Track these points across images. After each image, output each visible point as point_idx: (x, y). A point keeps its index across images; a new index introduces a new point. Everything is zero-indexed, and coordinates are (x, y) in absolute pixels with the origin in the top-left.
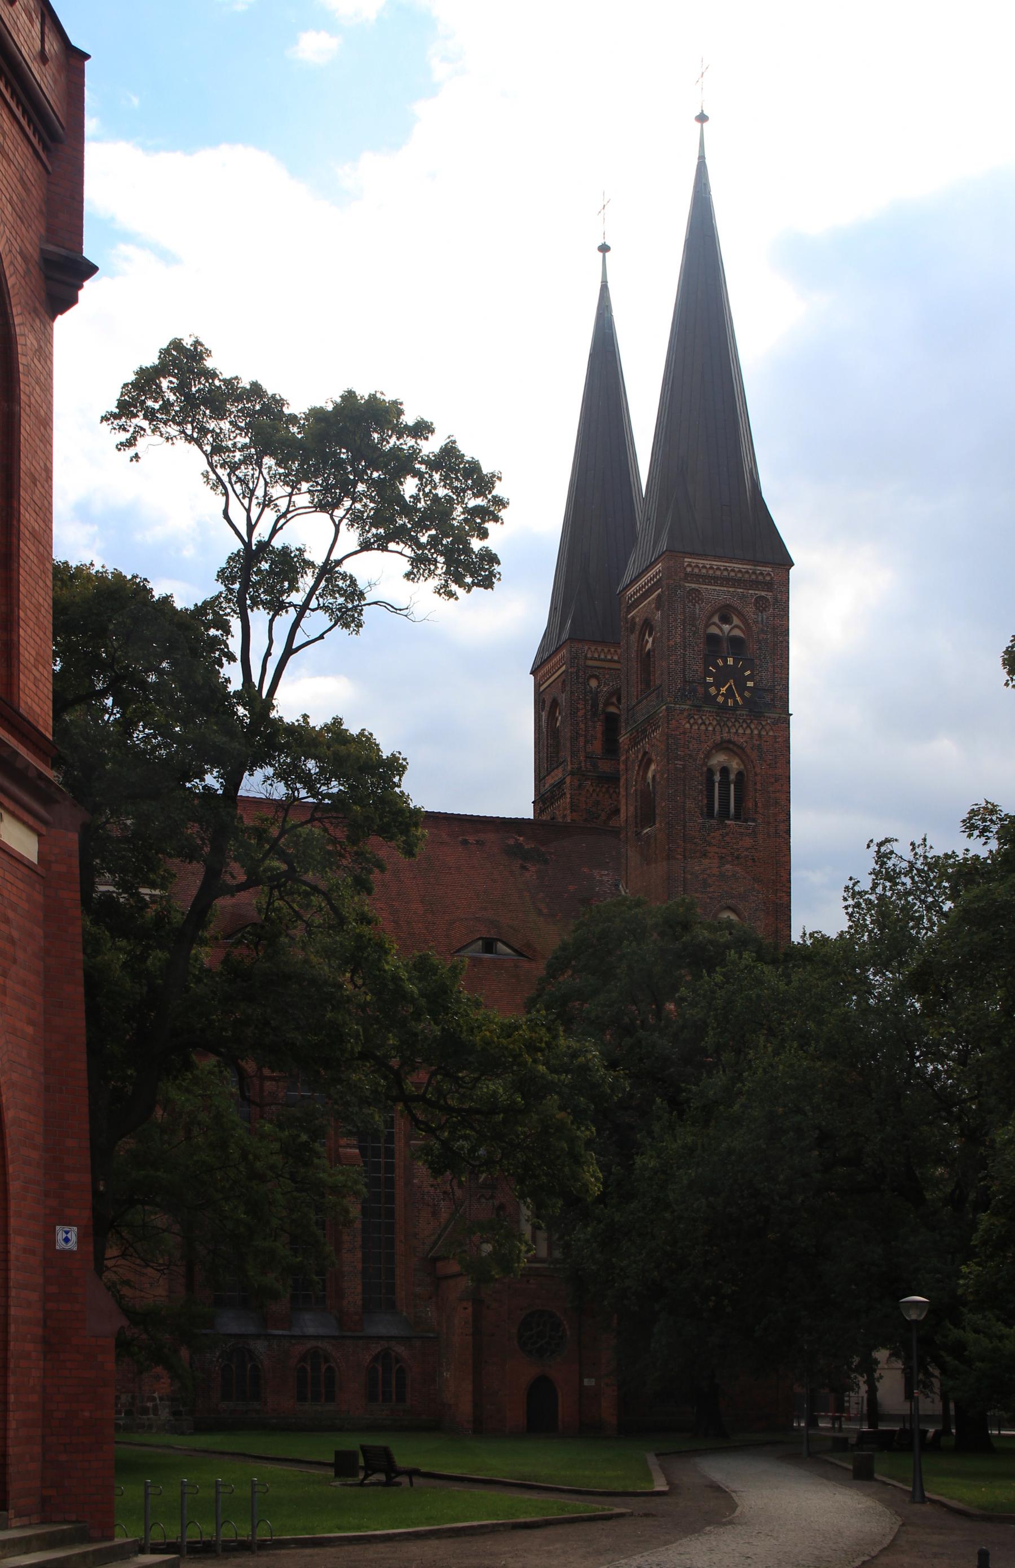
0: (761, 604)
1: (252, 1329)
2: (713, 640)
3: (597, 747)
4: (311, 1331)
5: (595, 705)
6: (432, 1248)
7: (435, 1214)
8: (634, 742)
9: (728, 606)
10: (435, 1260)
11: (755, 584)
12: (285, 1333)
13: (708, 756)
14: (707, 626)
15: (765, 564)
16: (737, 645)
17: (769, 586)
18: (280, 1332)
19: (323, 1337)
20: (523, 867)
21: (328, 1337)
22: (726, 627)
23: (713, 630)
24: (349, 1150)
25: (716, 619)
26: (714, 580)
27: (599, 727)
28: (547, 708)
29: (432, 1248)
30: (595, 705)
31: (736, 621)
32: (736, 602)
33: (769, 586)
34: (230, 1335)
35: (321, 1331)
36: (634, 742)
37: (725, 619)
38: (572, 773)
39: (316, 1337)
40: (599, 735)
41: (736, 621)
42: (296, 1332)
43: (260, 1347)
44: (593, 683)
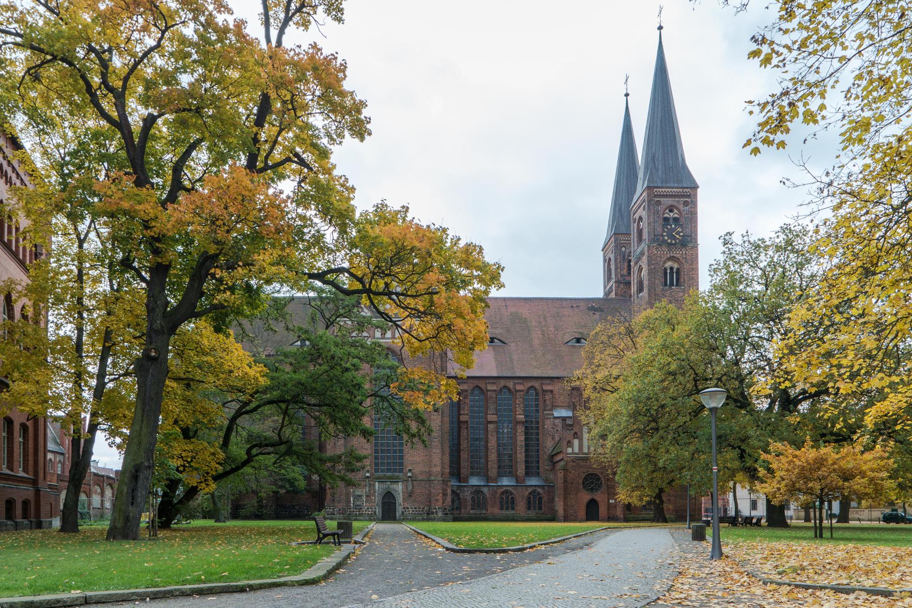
3: (625, 272)
4: (505, 484)
8: (636, 263)
9: (672, 206)
11: (683, 196)
13: (665, 263)
15: (687, 188)
16: (676, 220)
22: (671, 214)
26: (666, 196)
31: (676, 211)
32: (675, 204)
33: (689, 196)
35: (509, 484)
36: (636, 263)
37: (671, 211)
41: (676, 211)
44: (623, 249)
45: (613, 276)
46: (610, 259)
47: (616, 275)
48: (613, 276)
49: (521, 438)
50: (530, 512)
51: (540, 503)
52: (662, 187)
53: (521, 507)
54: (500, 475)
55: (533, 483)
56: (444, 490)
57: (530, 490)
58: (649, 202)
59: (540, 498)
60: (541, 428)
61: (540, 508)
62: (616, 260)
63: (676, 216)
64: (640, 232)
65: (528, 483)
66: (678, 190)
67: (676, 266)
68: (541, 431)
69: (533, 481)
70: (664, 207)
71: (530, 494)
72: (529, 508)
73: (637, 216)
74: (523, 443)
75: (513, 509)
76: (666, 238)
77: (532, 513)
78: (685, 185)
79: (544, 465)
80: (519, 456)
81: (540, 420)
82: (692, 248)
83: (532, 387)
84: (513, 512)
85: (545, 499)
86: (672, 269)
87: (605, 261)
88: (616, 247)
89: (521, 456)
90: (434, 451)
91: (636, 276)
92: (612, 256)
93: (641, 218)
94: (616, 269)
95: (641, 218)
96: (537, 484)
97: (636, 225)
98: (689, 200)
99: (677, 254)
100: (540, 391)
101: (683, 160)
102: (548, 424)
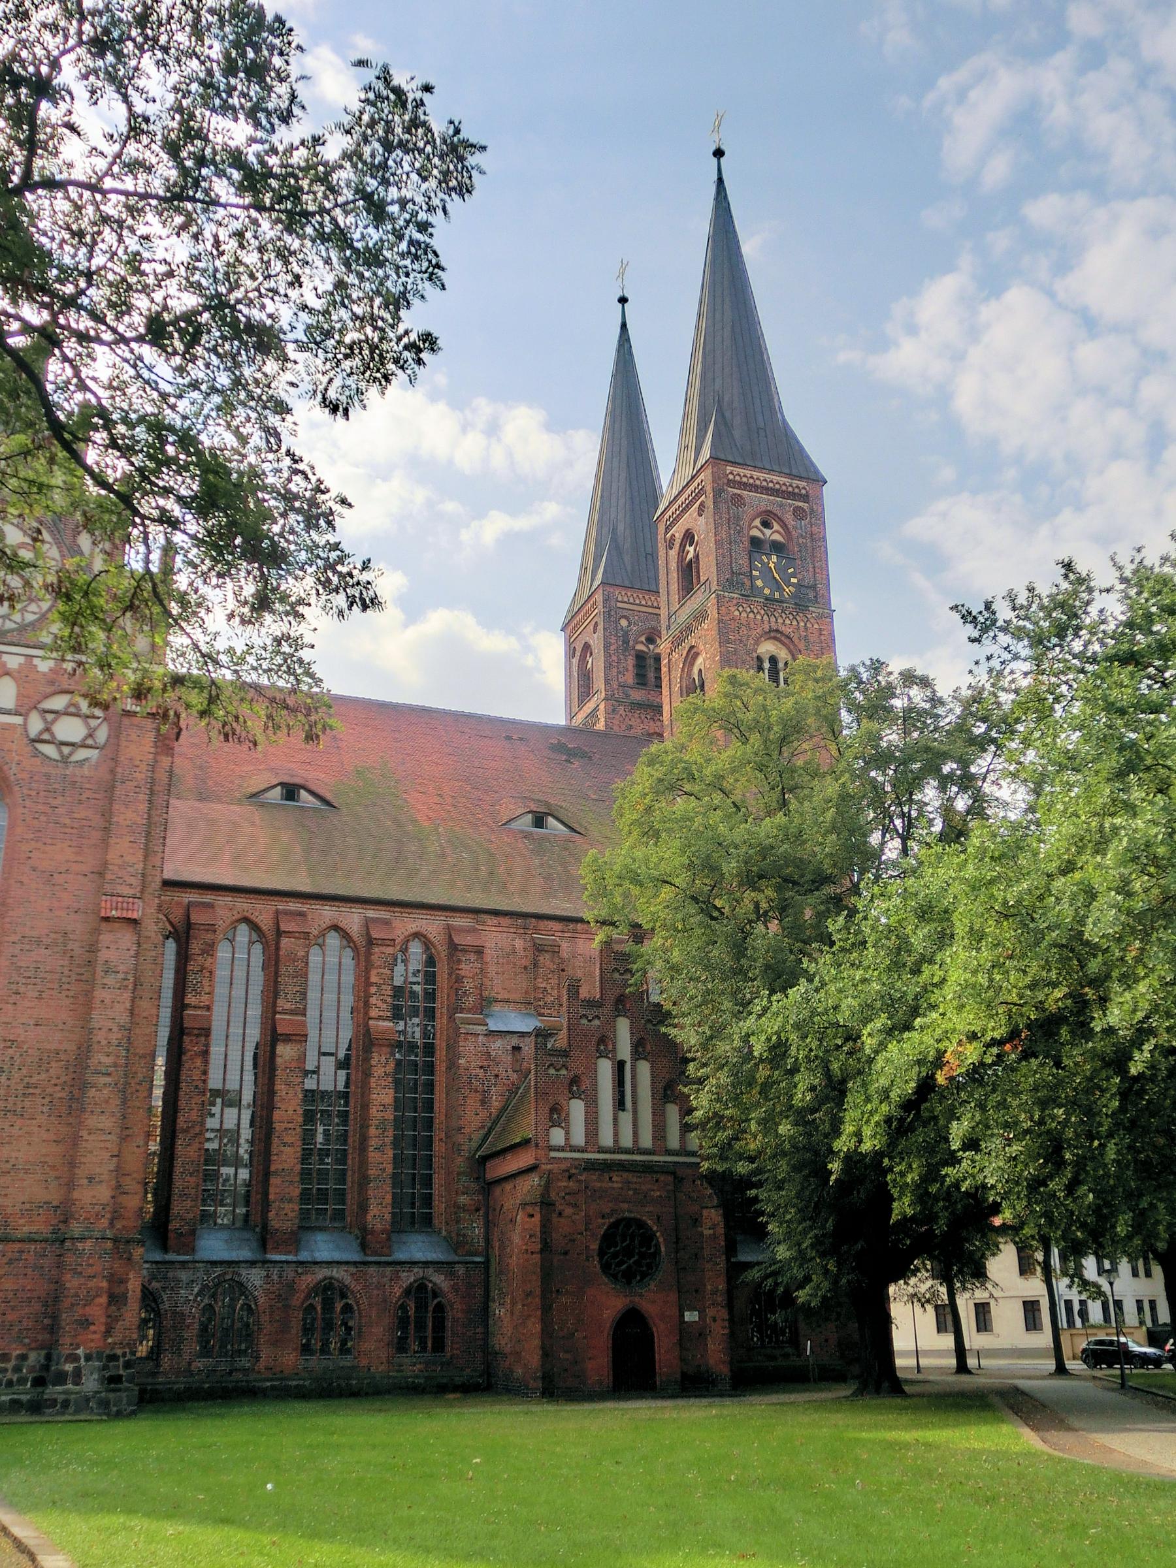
0: (799, 513)
1: (245, 1254)
2: (756, 542)
3: (629, 678)
5: (626, 642)
6: (481, 1146)
7: (483, 1102)
8: (677, 642)
9: (769, 512)
10: (485, 1159)
11: (792, 495)
12: (290, 1258)
14: (750, 528)
15: (801, 478)
16: (777, 547)
17: (805, 498)
18: (283, 1258)
19: (338, 1263)
20: (567, 761)
21: (347, 1263)
22: (768, 532)
23: (755, 532)
24: (381, 1023)
25: (757, 522)
26: (755, 488)
27: (631, 661)
28: (578, 654)
29: (481, 1146)
30: (626, 642)
31: (776, 527)
32: (776, 510)
33: (805, 498)
34: (214, 1263)
35: (337, 1256)
36: (677, 642)
37: (766, 524)
38: (606, 699)
39: (329, 1263)
40: (631, 668)
41: (776, 527)
42: (304, 1256)
43: (255, 1278)
44: (624, 623)
45: (599, 683)
46: (587, 647)
47: (607, 682)
48: (599, 683)
49: (382, 1096)
50: (405, 1359)
51: (439, 1325)
52: (744, 465)
53: (373, 1348)
54: (306, 1226)
55: (419, 1256)
56: (117, 1281)
57: (408, 1278)
58: (718, 493)
59: (440, 1308)
60: (441, 1067)
61: (439, 1346)
62: (607, 646)
63: (777, 537)
64: (689, 573)
65: (401, 1256)
66: (782, 480)
67: (783, 654)
68: (440, 1078)
69: (418, 1248)
70: (749, 511)
71: (407, 1292)
72: (401, 1346)
73: (678, 532)
74: (390, 1115)
75: (344, 1350)
76: (759, 583)
77: (413, 1366)
78: (794, 472)
79: (449, 1190)
80: (373, 1156)
81: (440, 1044)
82: (820, 616)
83: (416, 935)
84: (347, 1361)
85: (456, 1310)
86: (773, 660)
87: (571, 652)
88: (607, 615)
89: (381, 1158)
90: (92, 1121)
91: (677, 674)
92: (596, 641)
93: (689, 537)
94: (608, 668)
95: (689, 537)
96: (432, 1256)
97: (673, 553)
98: (805, 506)
99: (787, 625)
100: (442, 951)
101: (784, 420)
102: (469, 1055)
